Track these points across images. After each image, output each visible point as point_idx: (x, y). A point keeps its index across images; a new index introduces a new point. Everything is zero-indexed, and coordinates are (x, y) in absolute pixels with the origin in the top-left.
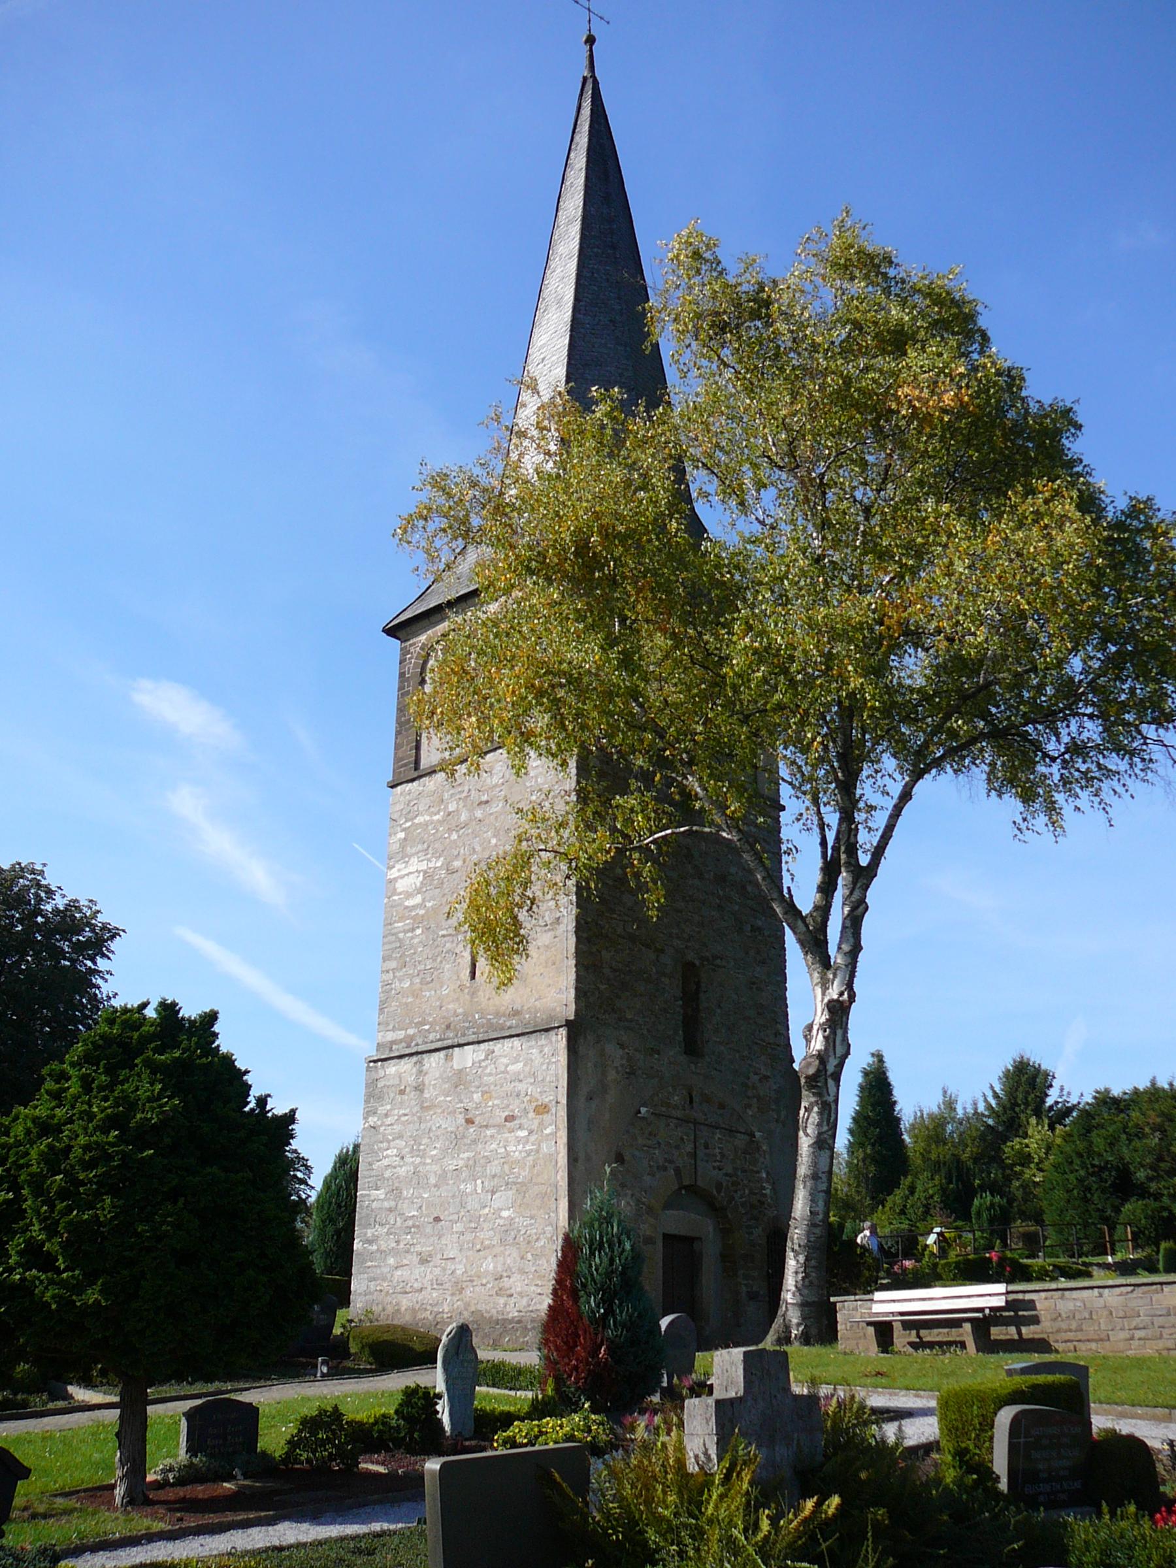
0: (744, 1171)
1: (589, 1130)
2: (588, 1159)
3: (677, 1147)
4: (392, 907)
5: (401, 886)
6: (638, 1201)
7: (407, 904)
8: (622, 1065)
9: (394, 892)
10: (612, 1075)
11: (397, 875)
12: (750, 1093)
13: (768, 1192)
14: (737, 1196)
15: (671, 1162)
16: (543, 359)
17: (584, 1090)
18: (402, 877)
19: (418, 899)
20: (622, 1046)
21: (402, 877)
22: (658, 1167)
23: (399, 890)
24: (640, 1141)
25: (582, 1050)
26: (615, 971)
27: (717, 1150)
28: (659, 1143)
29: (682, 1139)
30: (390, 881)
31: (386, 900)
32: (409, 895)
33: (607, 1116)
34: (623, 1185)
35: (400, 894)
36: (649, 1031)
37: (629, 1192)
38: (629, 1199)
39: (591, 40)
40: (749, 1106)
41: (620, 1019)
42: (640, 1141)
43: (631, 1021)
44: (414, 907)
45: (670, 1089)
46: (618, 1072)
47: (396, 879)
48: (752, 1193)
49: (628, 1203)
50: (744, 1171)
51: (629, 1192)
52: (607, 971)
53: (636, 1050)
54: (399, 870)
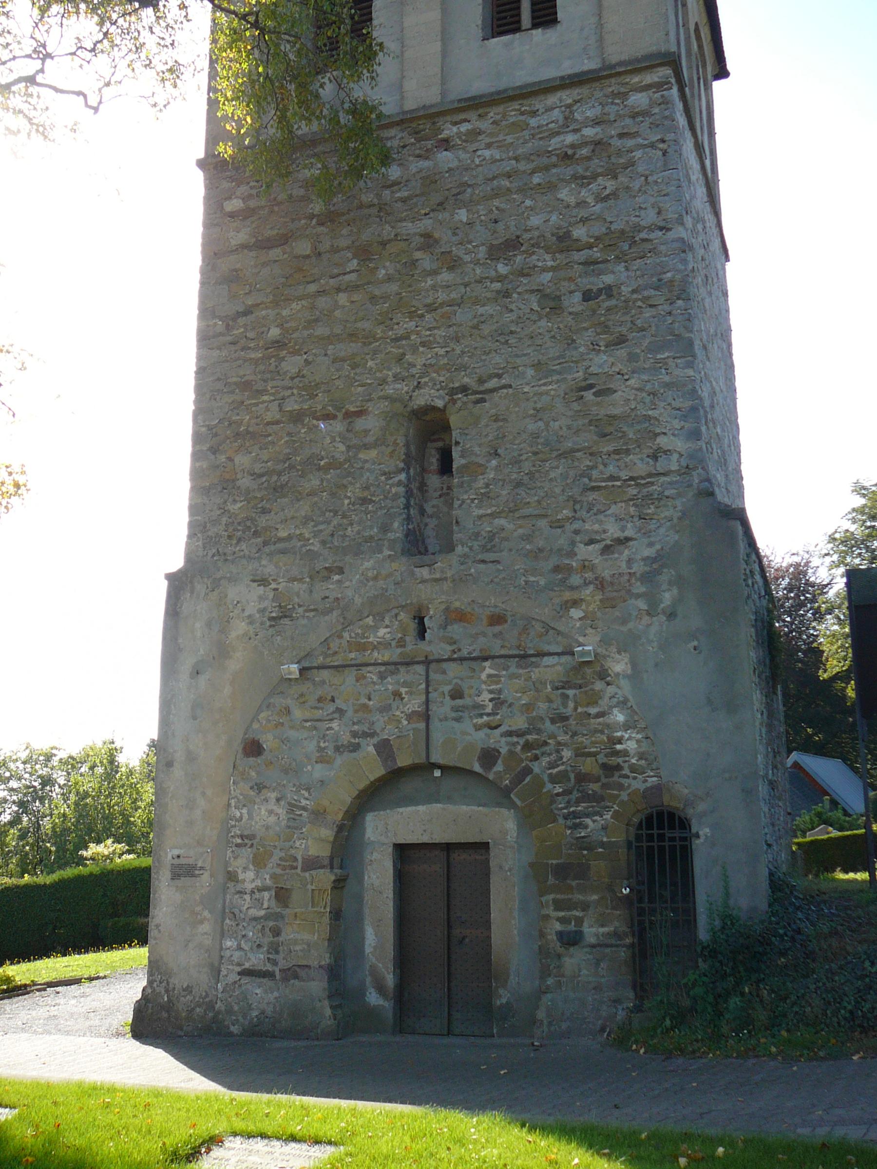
0: (560, 719)
1: (195, 718)
2: (191, 757)
3: (385, 709)
6: (292, 807)
8: (262, 611)
10: (240, 627)
12: (576, 580)
13: (631, 746)
14: (536, 767)
15: (365, 735)
17: (187, 663)
20: (263, 582)
22: (337, 749)
24: (298, 714)
25: (186, 608)
26: (261, 475)
27: (486, 696)
28: (340, 711)
29: (397, 695)
33: (227, 690)
34: (259, 787)
36: (323, 543)
37: (273, 795)
38: (272, 805)
40: (575, 603)
41: (265, 543)
42: (298, 714)
43: (289, 538)
45: (370, 621)
46: (251, 623)
48: (580, 753)
49: (271, 812)
50: (560, 719)
51: (273, 795)
52: (245, 482)
53: (293, 580)
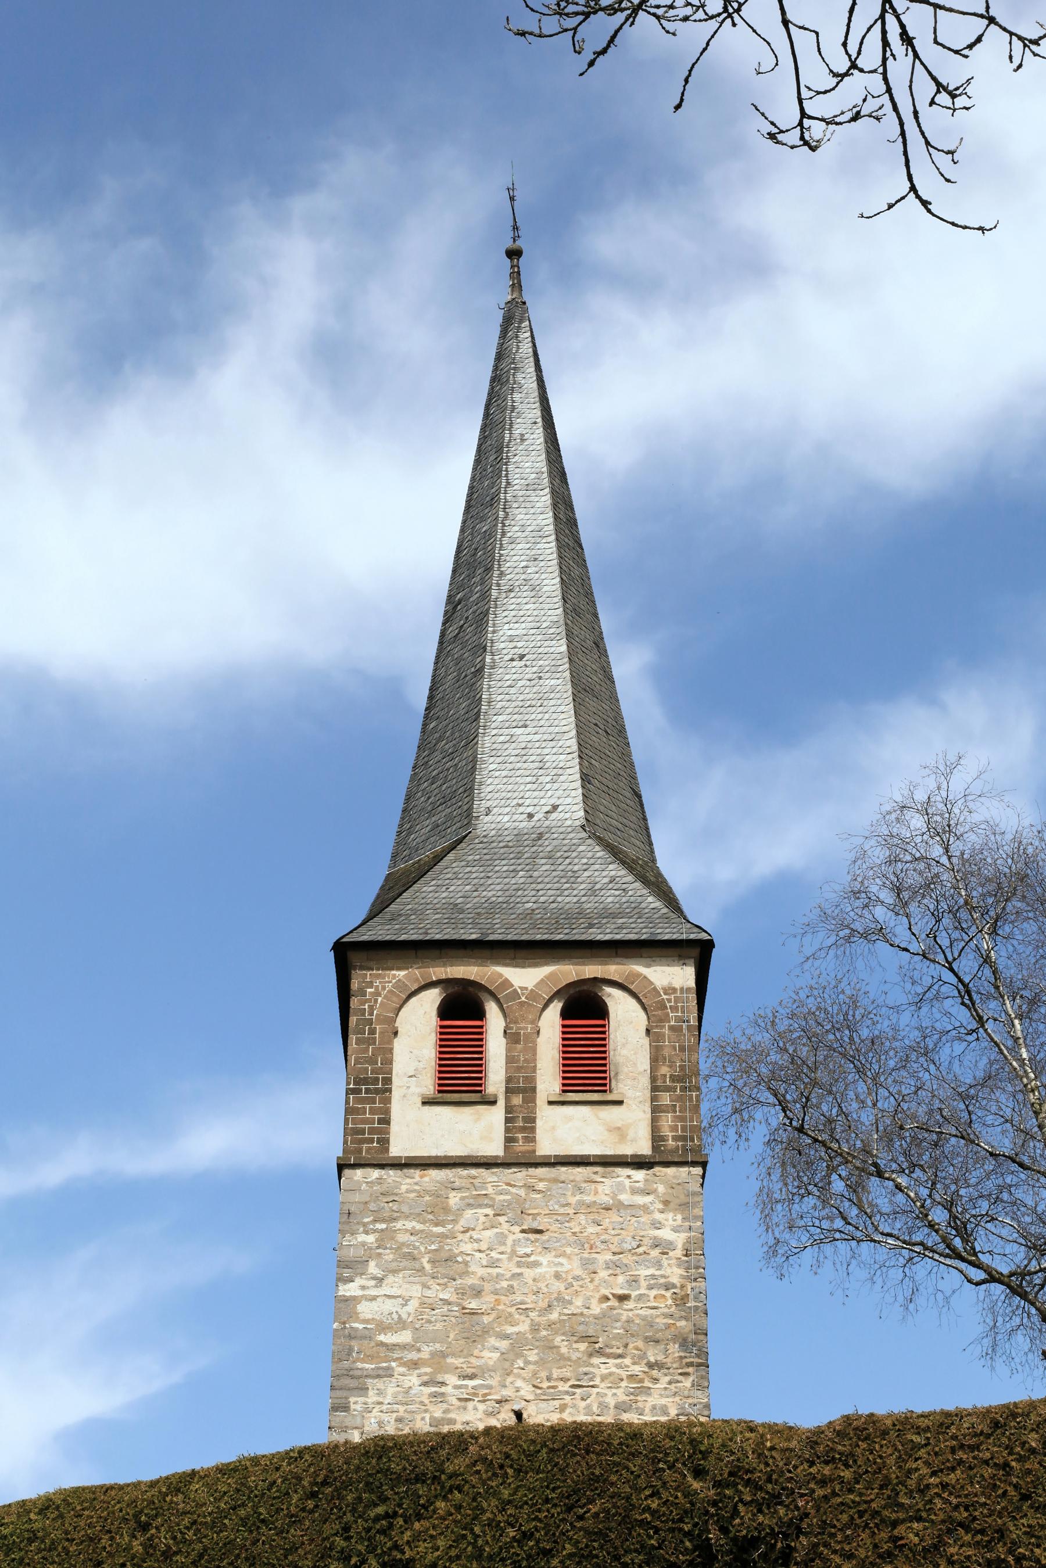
4: (350, 1337)
5: (365, 1309)
7: (382, 1338)
9: (354, 1316)
11: (360, 1293)
16: (522, 657)
18: (374, 1298)
19: (405, 1337)
21: (374, 1298)
23: (362, 1316)
30: (346, 1300)
31: (336, 1325)
32: (383, 1328)
35: (367, 1321)
39: (514, 254)
44: (396, 1346)
47: (355, 1300)
54: (363, 1288)
